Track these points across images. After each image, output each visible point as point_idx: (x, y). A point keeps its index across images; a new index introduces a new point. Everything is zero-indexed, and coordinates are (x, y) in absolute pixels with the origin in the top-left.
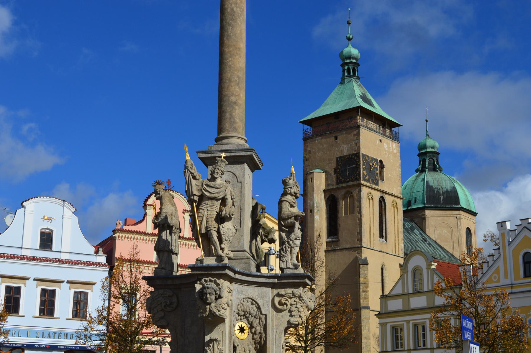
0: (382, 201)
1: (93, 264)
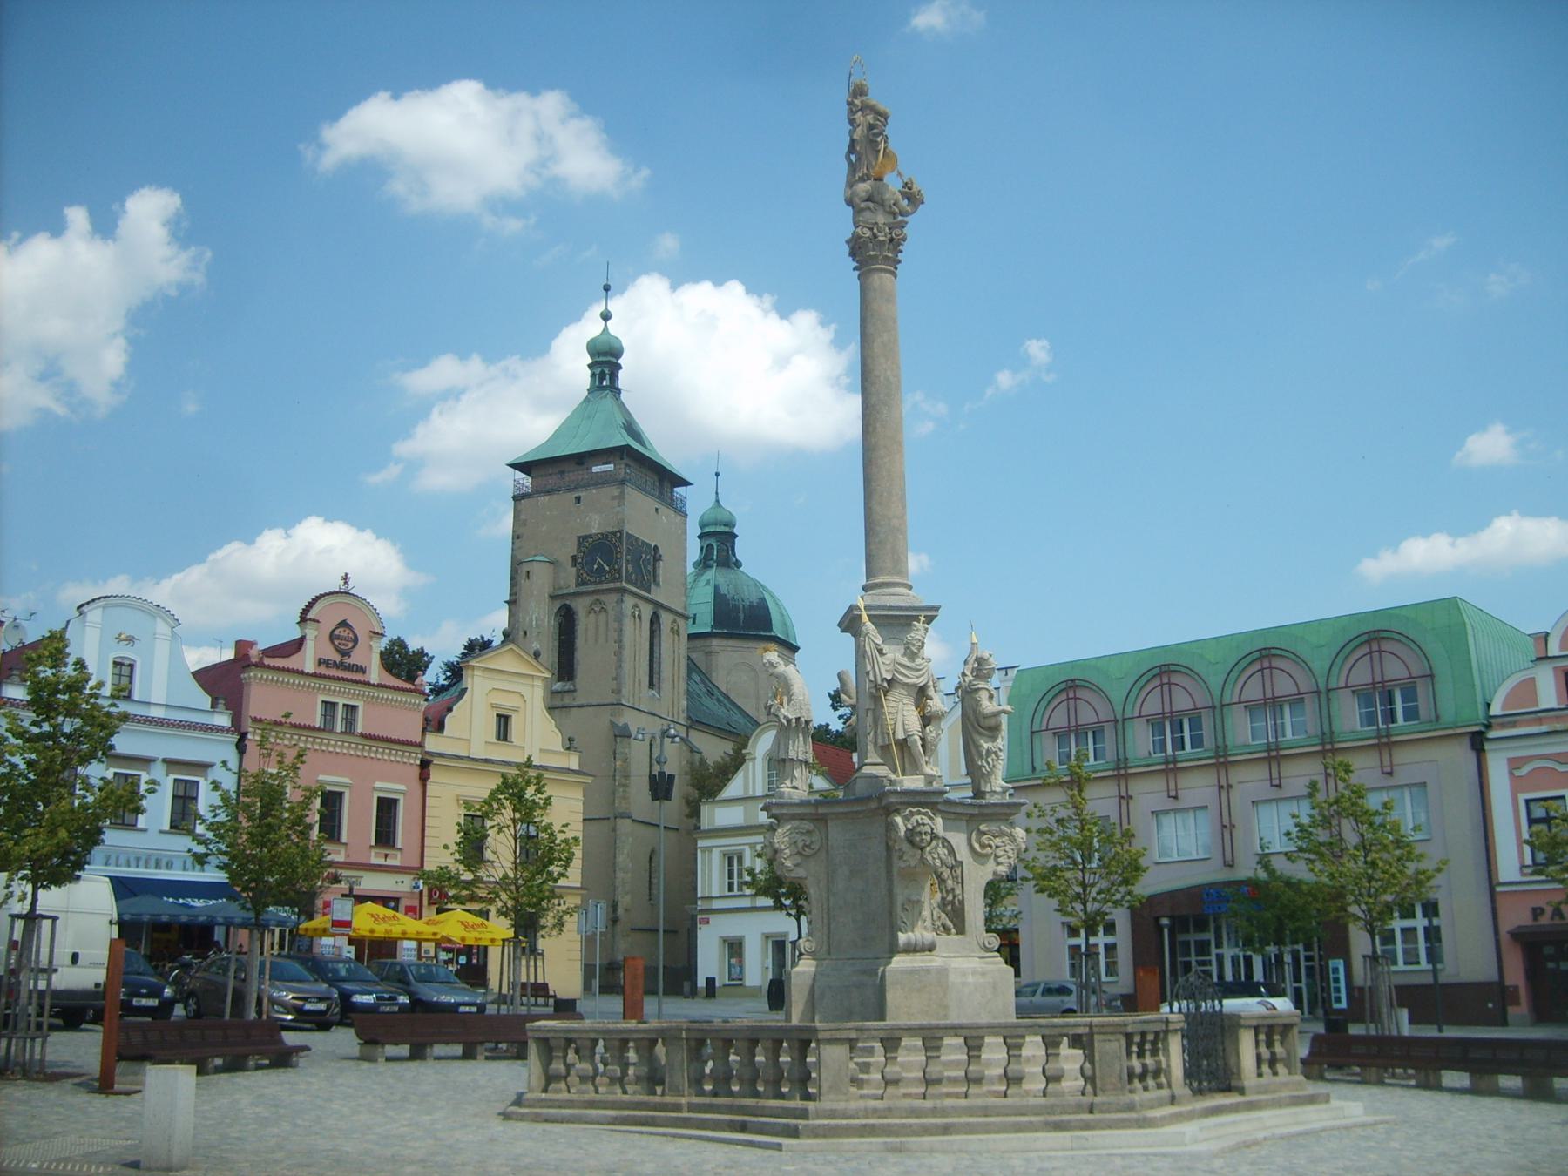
0: (655, 620)
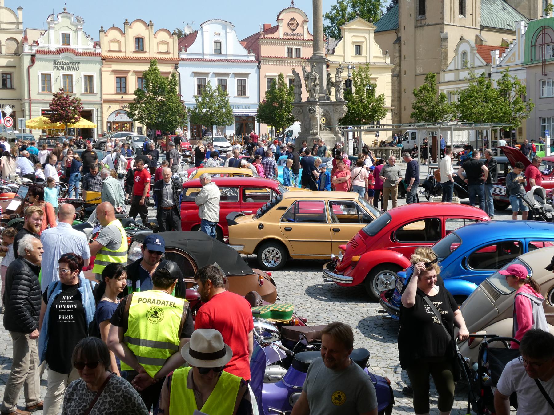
1: (248, 61)
